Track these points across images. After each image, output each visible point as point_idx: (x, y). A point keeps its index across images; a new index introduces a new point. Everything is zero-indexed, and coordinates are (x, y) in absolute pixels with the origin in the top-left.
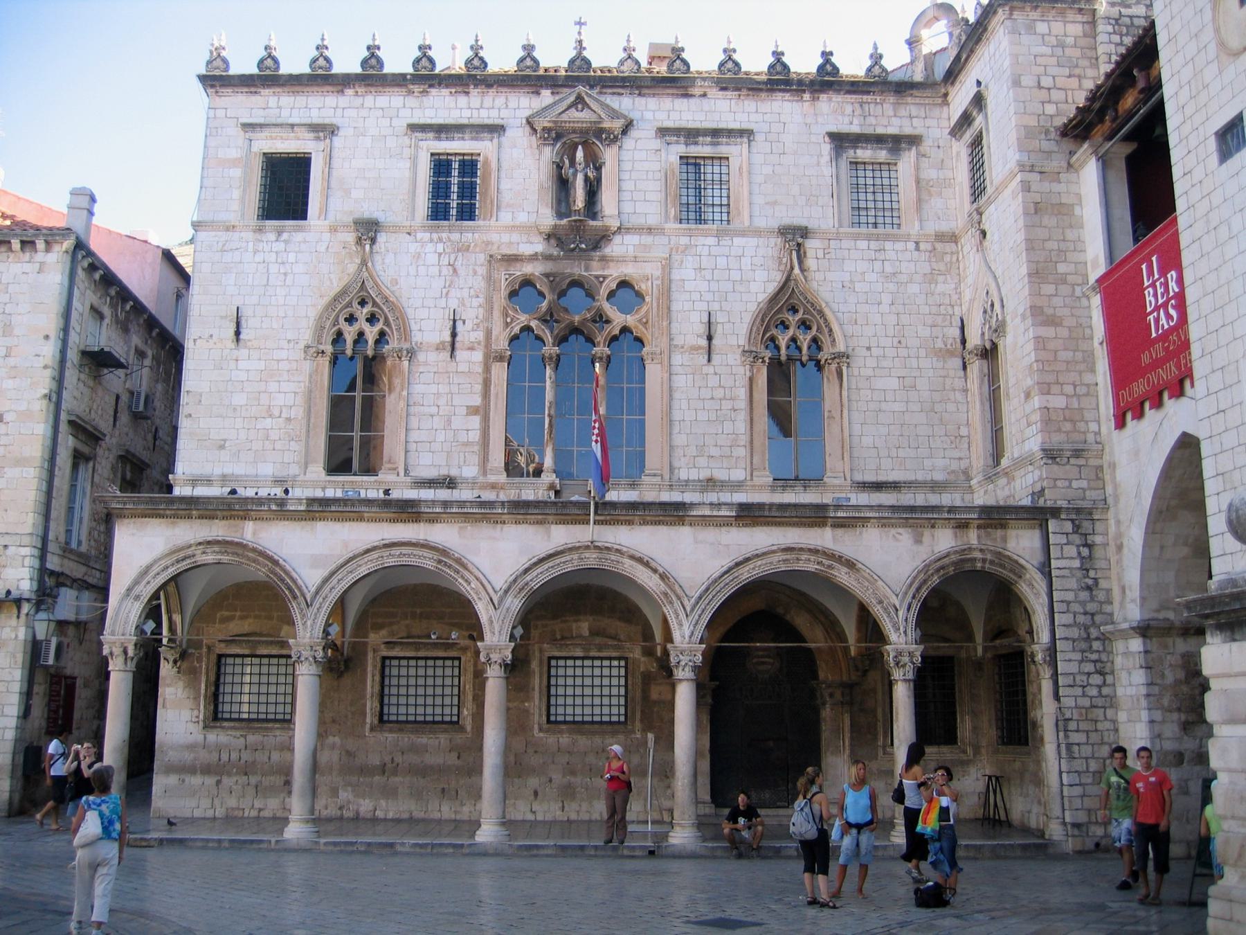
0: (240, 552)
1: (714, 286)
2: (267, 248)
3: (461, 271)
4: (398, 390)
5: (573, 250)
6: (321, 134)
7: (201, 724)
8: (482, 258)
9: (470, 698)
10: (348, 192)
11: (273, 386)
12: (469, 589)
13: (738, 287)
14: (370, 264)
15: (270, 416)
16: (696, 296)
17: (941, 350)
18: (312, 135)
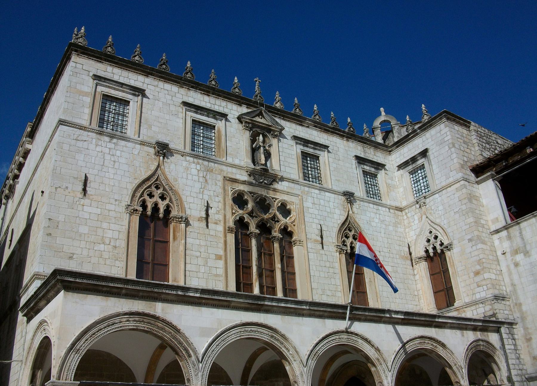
0: (152, 322)
3: (209, 181)
4: (179, 239)
5: (262, 182)
6: (137, 93)
8: (220, 178)
10: (150, 127)
11: (105, 225)
13: (330, 215)
14: (162, 167)
15: (104, 243)
16: (314, 216)
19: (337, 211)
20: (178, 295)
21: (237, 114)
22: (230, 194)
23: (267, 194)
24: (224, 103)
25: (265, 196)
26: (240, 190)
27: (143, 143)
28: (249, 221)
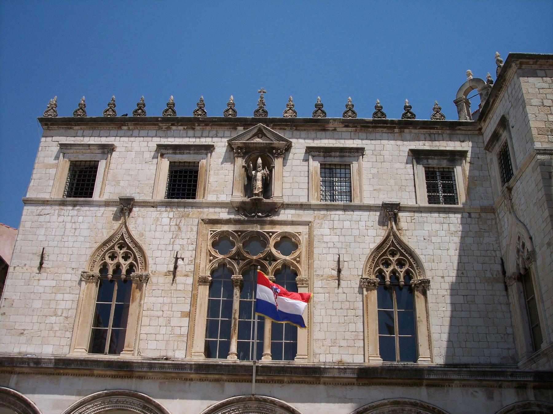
1: (342, 239)
2: (66, 214)
3: (184, 228)
5: (254, 216)
10: (118, 182)
11: (59, 296)
15: (56, 315)
16: (331, 245)
17: (489, 278)
18: (100, 151)
19: (372, 232)
27: (107, 204)
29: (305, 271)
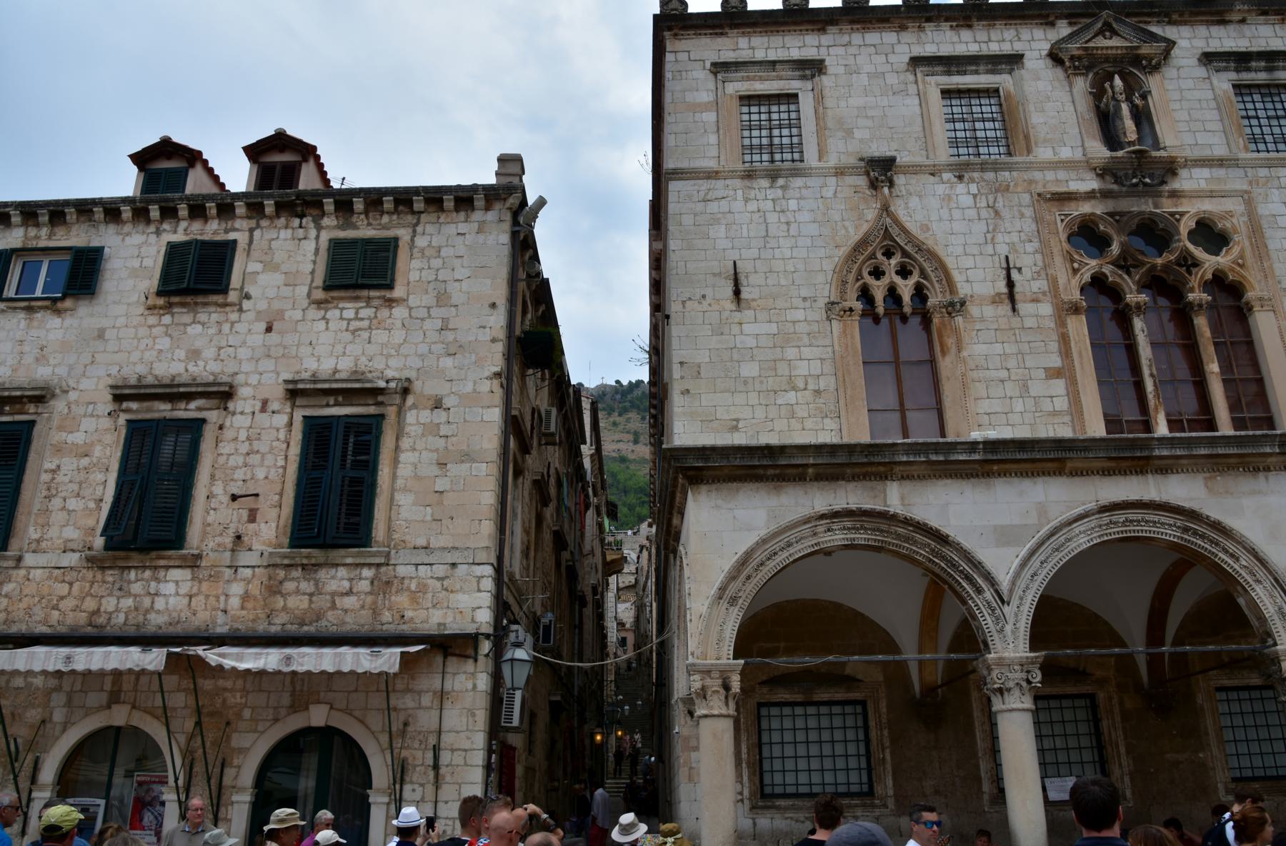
0: (884, 527)
3: (1005, 213)
4: (953, 350)
5: (1136, 185)
6: (808, 72)
7: (747, 802)
8: (1026, 198)
9: (1123, 750)
10: (849, 133)
11: (791, 353)
12: (1240, 567)
14: (892, 209)
15: (794, 389)
18: (797, 73)
20: (929, 462)
21: (1046, 47)
22: (1061, 229)
23: (1156, 206)
24: (1009, 33)
25: (1151, 213)
26: (1084, 215)
27: (840, 172)
28: (1118, 280)
29: (1259, 282)
